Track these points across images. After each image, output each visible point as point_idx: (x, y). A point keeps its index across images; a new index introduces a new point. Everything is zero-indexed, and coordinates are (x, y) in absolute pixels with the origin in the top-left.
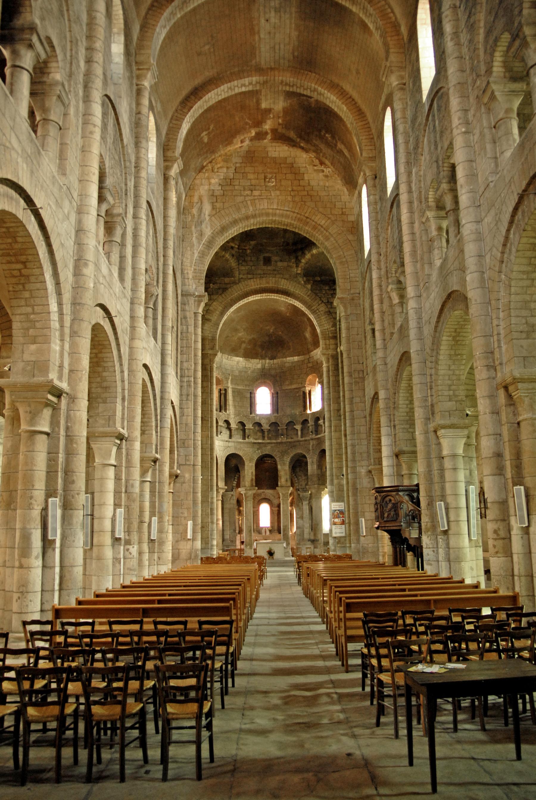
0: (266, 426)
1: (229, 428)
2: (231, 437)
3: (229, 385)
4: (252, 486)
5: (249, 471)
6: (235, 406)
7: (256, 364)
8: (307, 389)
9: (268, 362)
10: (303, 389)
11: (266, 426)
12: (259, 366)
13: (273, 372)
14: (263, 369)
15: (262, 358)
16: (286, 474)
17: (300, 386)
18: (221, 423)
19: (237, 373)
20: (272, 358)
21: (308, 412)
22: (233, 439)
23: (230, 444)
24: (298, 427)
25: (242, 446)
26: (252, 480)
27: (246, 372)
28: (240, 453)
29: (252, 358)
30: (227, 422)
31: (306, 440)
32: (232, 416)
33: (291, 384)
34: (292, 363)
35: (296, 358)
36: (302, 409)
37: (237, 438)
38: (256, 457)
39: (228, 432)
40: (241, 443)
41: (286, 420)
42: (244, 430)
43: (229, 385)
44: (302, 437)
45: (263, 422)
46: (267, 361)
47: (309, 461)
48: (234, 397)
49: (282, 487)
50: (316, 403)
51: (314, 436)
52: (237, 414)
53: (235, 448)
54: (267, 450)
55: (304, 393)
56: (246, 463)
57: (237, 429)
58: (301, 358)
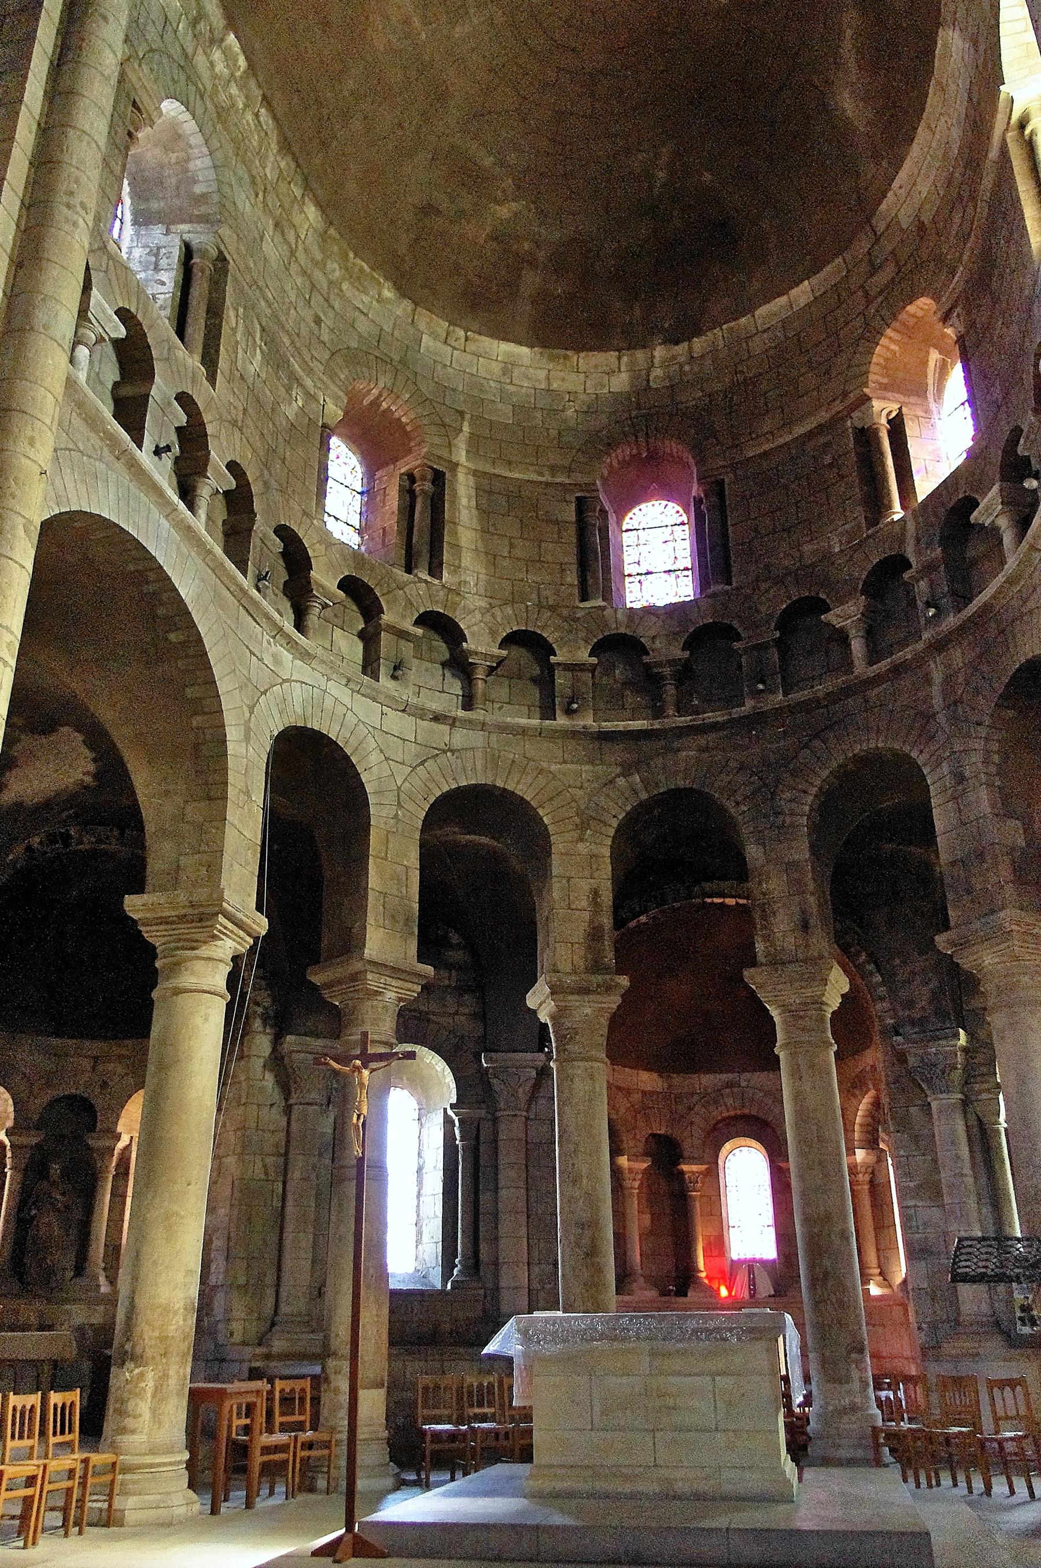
0: (665, 650)
1: (459, 664)
2: (468, 703)
3: (461, 456)
4: (596, 967)
5: (577, 885)
6: (492, 559)
7: (597, 377)
8: (882, 409)
9: (660, 358)
10: (856, 419)
11: (665, 650)
12: (621, 382)
13: (691, 398)
14: (642, 389)
15: (633, 339)
16: (797, 886)
17: (838, 406)
19: (504, 413)
20: (681, 333)
21: (897, 513)
24: (846, 615)
25: (530, 748)
26: (595, 934)
28: (523, 787)
29: (581, 347)
30: (440, 625)
31: (897, 670)
33: (788, 424)
34: (785, 323)
35: (802, 293)
36: (860, 513)
38: (615, 813)
39: (456, 687)
40: (524, 731)
41: (776, 602)
42: (545, 682)
43: (461, 456)
44: (874, 655)
45: (645, 633)
46: (660, 352)
47: (937, 782)
48: (485, 513)
49: (776, 962)
50: (943, 439)
51: (951, 621)
53: (493, 759)
54: (679, 768)
55: (866, 437)
56: (559, 844)
58: (831, 272)
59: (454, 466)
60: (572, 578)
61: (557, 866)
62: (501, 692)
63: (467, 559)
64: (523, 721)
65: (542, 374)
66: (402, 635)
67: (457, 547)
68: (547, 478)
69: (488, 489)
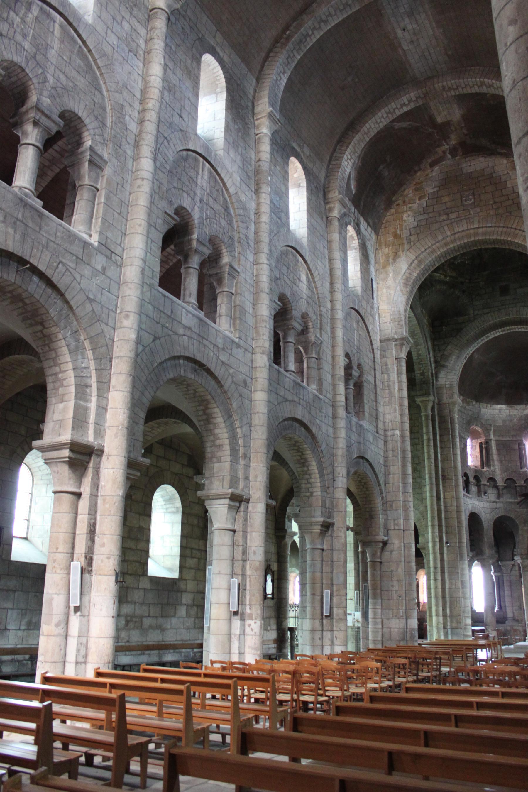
1: (496, 487)
2: (499, 496)
3: (492, 437)
6: (501, 461)
18: (484, 482)
22: (501, 500)
23: (498, 505)
27: (511, 421)
28: (512, 516)
30: (492, 479)
32: (498, 473)
37: (508, 498)
39: (495, 492)
40: (511, 503)
43: (492, 437)
48: (498, 450)
52: (503, 471)
56: (520, 527)
57: (505, 487)
59: (491, 440)
60: (519, 464)
61: (520, 532)
62: (505, 491)
63: (496, 463)
64: (511, 500)
65: (508, 411)
66: (485, 485)
67: (493, 460)
68: (511, 439)
69: (498, 443)
